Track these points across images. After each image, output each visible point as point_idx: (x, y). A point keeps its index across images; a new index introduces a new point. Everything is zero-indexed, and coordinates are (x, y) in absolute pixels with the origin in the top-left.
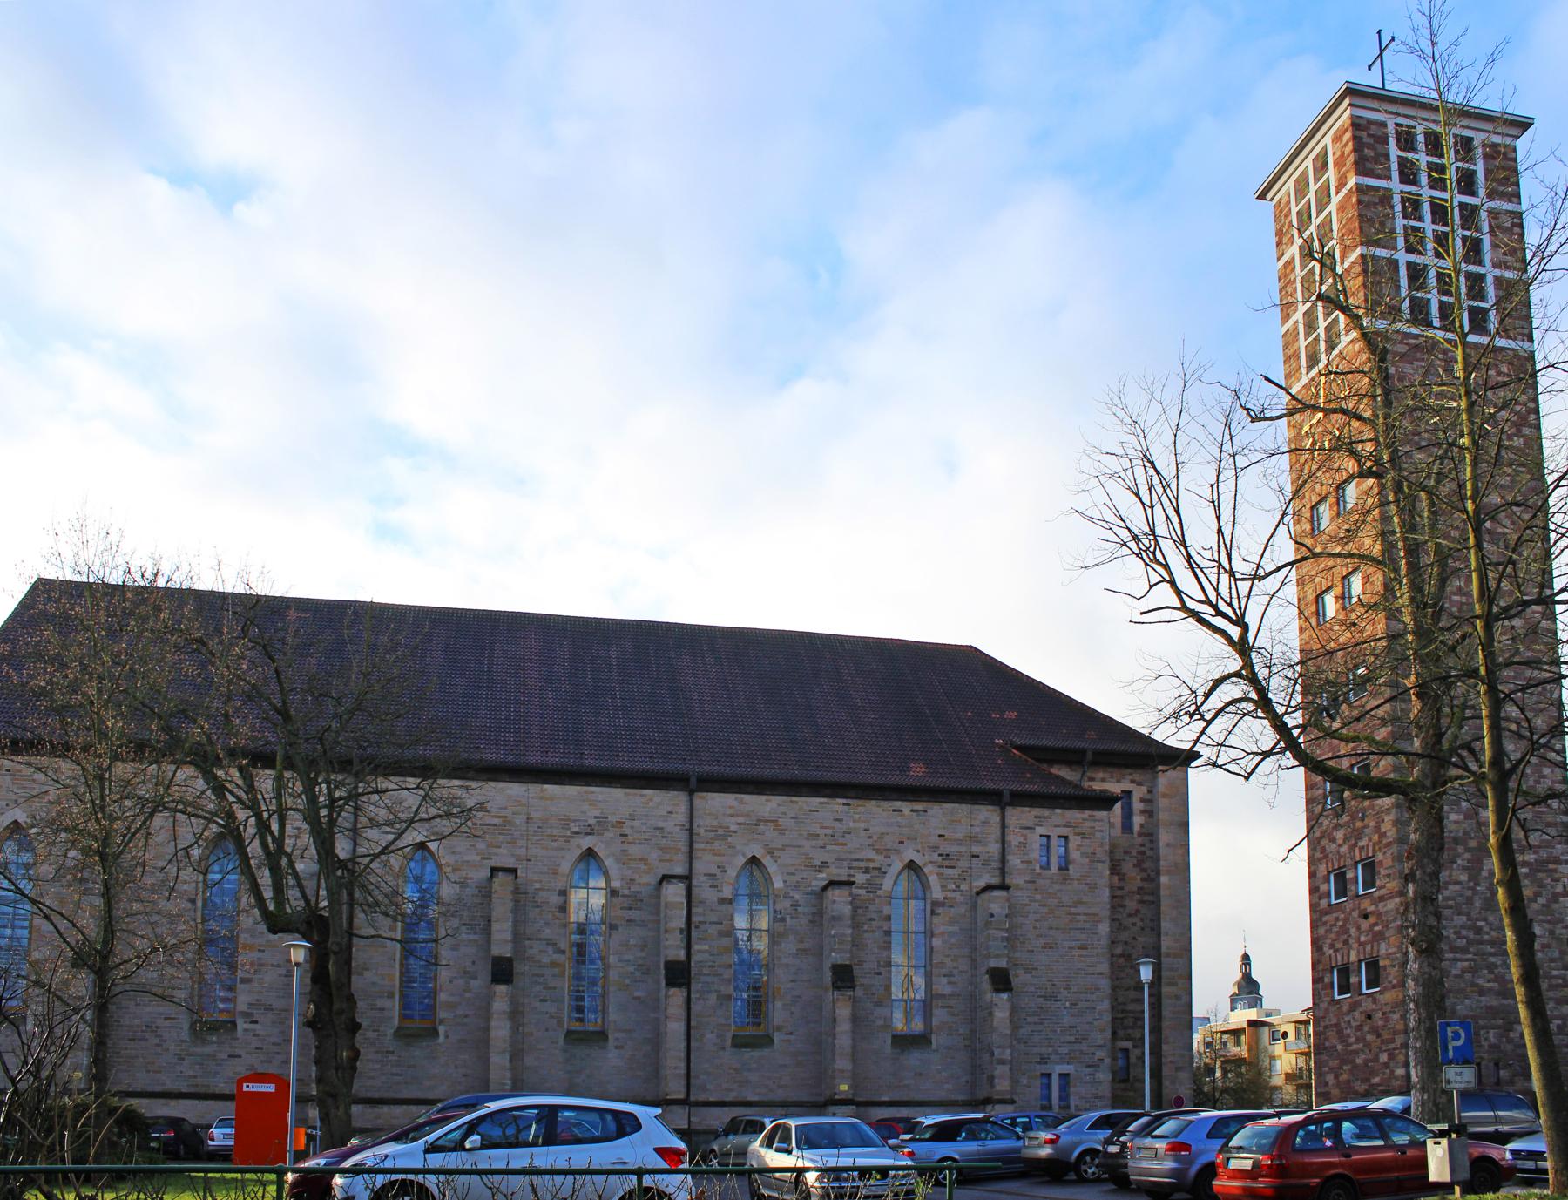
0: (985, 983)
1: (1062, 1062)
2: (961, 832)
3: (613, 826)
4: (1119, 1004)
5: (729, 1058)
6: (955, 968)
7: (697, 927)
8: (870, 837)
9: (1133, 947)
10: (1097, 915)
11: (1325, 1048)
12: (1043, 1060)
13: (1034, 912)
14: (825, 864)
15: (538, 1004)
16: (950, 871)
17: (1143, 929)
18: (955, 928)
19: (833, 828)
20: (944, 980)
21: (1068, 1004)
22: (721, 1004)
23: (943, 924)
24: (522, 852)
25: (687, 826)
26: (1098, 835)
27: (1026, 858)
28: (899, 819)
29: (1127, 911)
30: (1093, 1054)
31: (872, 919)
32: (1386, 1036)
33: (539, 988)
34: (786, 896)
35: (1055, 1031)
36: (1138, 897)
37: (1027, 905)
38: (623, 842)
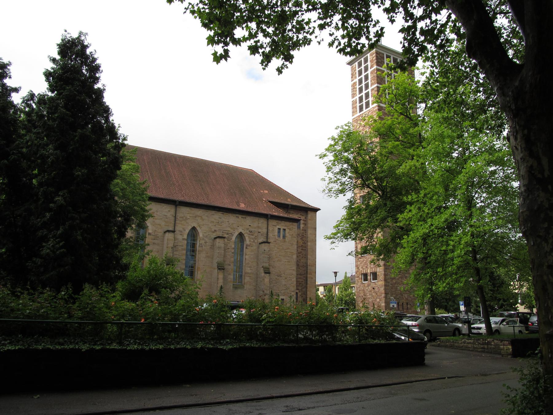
0: (262, 270)
11: (360, 296)
14: (215, 231)
16: (252, 236)
18: (253, 253)
20: (249, 268)
25: (174, 215)
26: (294, 229)
32: (378, 294)
34: (203, 239)
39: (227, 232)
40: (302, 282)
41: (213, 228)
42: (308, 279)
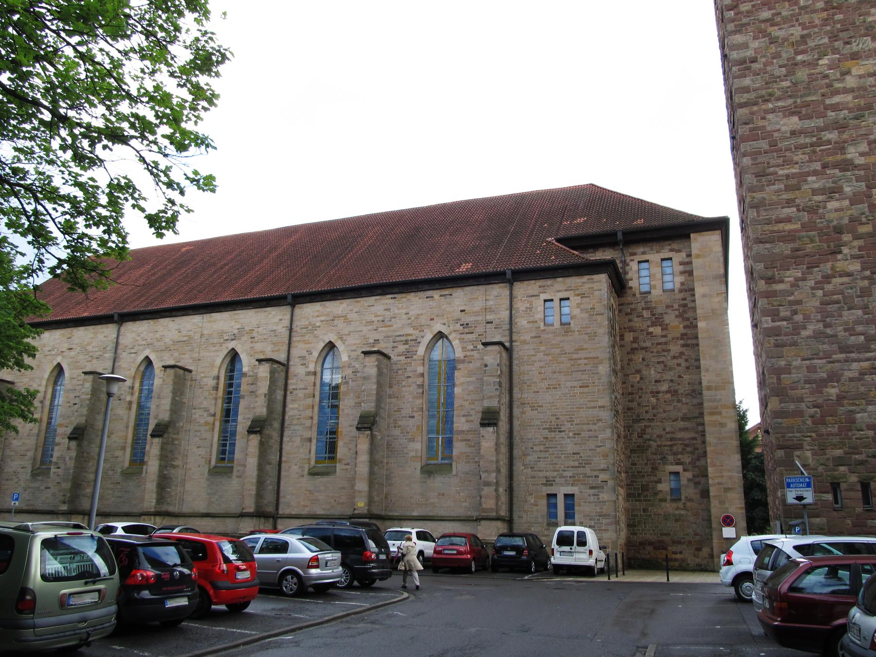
1: (567, 484)
2: (478, 305)
3: (247, 333)
4: (667, 433)
5: (307, 483)
6: (472, 409)
7: (291, 393)
8: (409, 319)
9: (679, 384)
10: (598, 358)
12: (549, 482)
13: (539, 361)
15: (195, 450)
16: (470, 336)
17: (688, 368)
18: (473, 379)
19: (384, 315)
20: (463, 419)
21: (571, 434)
22: (303, 445)
23: (462, 376)
24: (196, 355)
26: (596, 293)
27: (531, 319)
28: (431, 303)
29: (672, 353)
30: (597, 477)
31: (408, 377)
33: (197, 439)
35: (560, 457)
36: (682, 342)
37: (533, 355)
38: (252, 342)
39: (403, 338)
40: (695, 439)
42: (707, 429)
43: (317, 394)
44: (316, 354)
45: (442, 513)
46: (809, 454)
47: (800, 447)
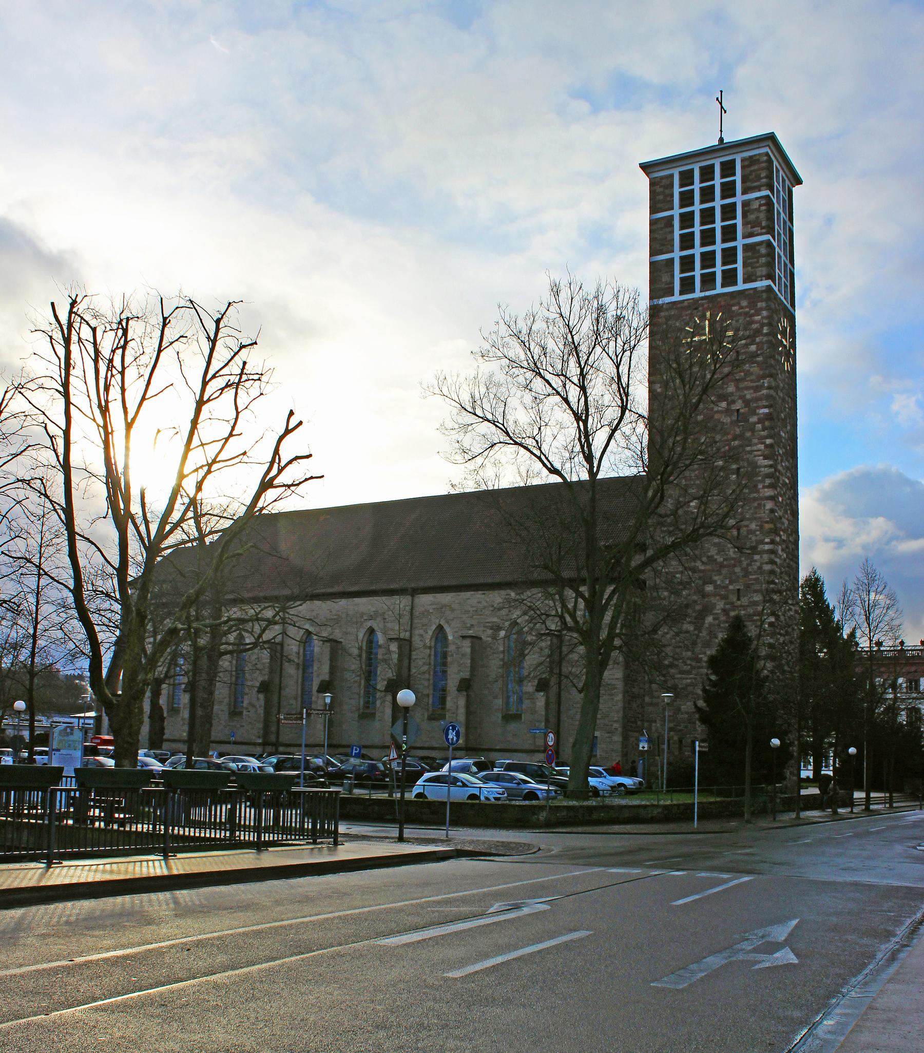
14: (472, 625)
24: (345, 630)
41: (469, 622)
43: (432, 663)
44: (430, 633)
45: (515, 747)
46: (658, 725)
47: (655, 722)
